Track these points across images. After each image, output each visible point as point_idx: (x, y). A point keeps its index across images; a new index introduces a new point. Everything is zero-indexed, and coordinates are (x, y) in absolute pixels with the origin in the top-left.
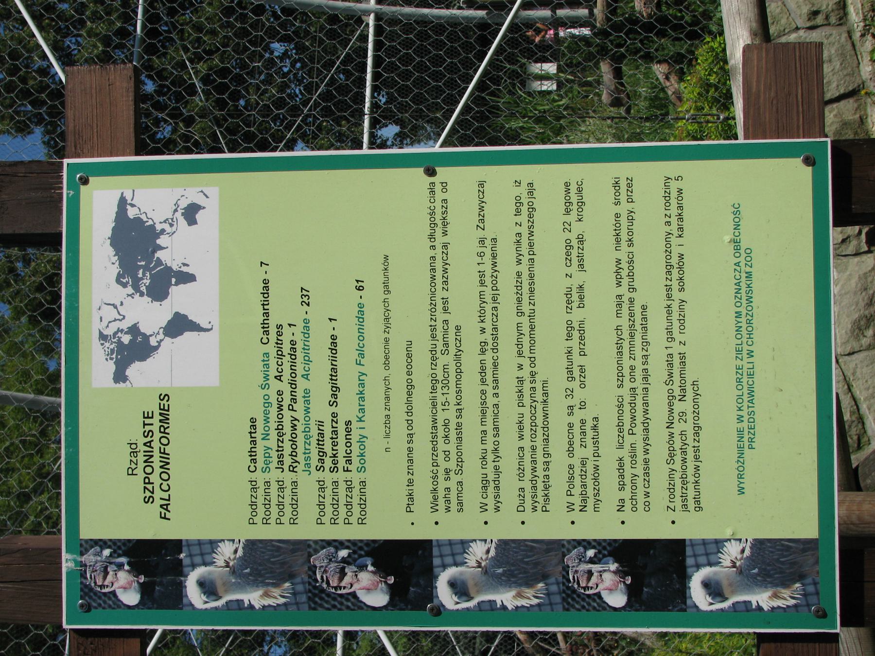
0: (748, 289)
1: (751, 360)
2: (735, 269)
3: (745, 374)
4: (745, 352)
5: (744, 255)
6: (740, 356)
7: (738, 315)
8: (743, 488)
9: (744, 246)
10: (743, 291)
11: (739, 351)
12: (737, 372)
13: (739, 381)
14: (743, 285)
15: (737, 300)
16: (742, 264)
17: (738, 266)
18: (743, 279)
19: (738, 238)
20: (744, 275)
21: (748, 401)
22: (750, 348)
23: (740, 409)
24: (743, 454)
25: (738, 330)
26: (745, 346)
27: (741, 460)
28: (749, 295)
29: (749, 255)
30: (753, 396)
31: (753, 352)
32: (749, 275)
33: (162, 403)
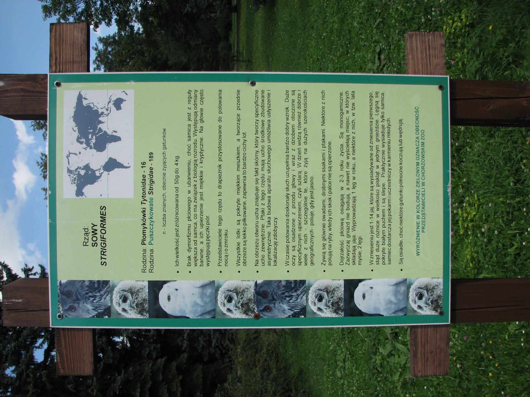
1: (423, 187)
3: (421, 194)
4: (421, 183)
5: (420, 133)
6: (418, 185)
7: (418, 164)
9: (421, 128)
10: (420, 152)
11: (418, 183)
13: (418, 198)
14: (420, 149)
15: (417, 156)
16: (420, 138)
18: (420, 146)
20: (420, 144)
22: (423, 181)
23: (418, 212)
25: (418, 171)
26: (421, 181)
29: (423, 133)
32: (423, 144)
33: (102, 211)
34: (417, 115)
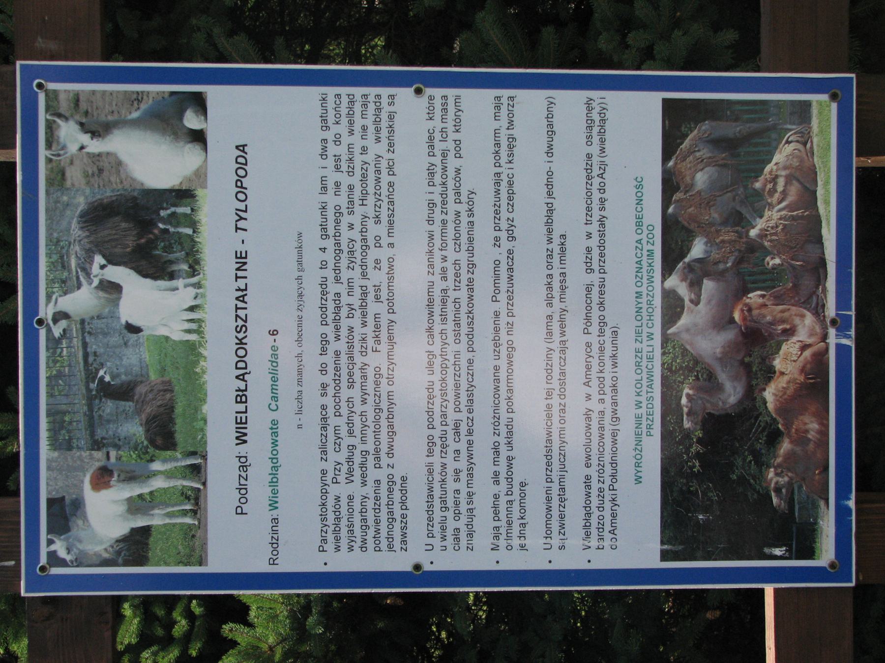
0: (650, 268)
1: (650, 343)
2: (636, 247)
4: (644, 335)
5: (646, 232)
6: (639, 339)
7: (639, 295)
8: (641, 477)
10: (644, 270)
11: (638, 333)
12: (636, 355)
13: (638, 365)
14: (645, 264)
16: (644, 242)
17: (640, 243)
18: (645, 258)
19: (640, 214)
20: (645, 253)
21: (647, 386)
24: (641, 441)
25: (639, 311)
26: (645, 330)
27: (639, 447)
28: (650, 274)
30: (652, 380)
31: (652, 334)
34: (639, 194)
